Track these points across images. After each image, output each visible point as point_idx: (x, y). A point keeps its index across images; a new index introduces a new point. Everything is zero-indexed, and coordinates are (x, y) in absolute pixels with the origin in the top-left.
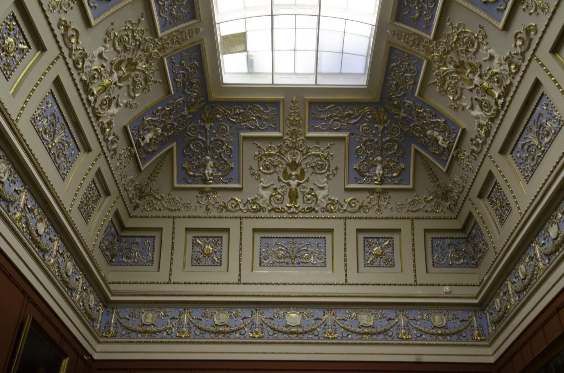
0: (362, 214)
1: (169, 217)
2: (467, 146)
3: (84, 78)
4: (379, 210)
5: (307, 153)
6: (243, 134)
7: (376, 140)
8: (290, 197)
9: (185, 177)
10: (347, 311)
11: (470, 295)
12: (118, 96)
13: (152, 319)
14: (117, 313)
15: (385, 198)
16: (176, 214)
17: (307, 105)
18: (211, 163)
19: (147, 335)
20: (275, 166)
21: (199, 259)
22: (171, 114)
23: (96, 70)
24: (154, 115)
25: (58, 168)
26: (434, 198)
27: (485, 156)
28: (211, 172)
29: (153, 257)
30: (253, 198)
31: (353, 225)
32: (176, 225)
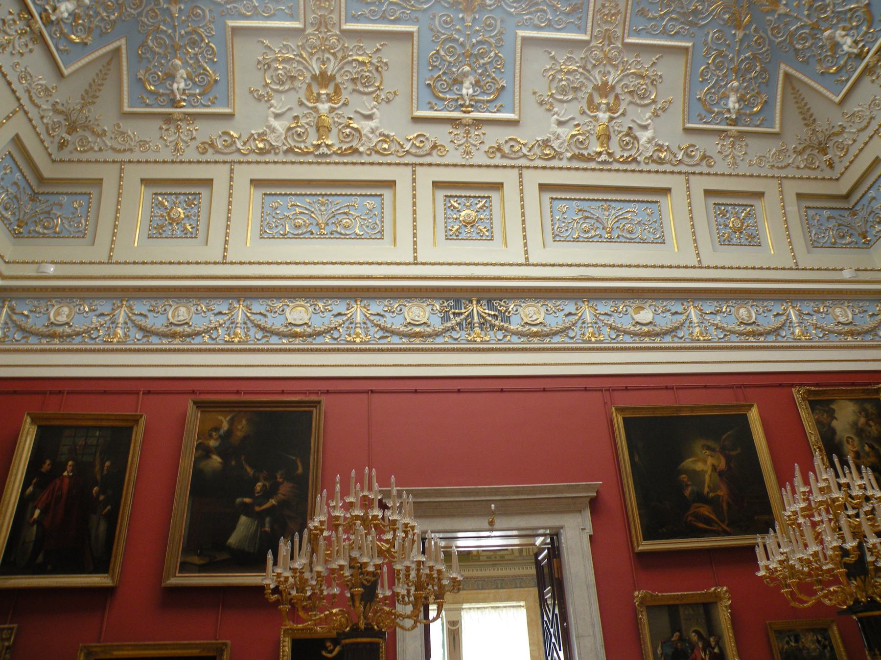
1: (114, 162)
5: (344, 58)
13: (68, 316)
14: (12, 309)
16: (126, 157)
19: (56, 341)
29: (86, 225)
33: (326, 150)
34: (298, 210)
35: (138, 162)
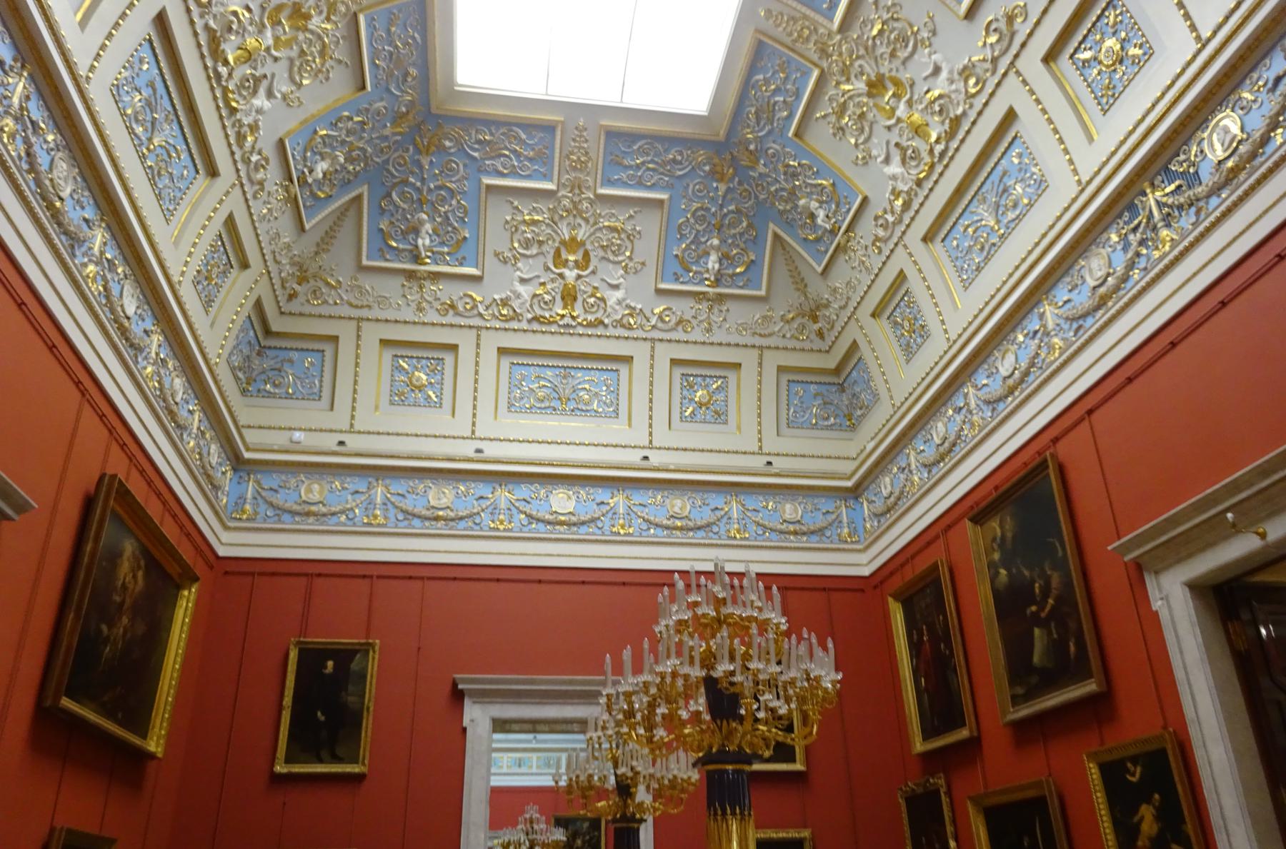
1: (350, 318)
2: (867, 229)
3: (212, 23)
4: (709, 330)
5: (595, 223)
6: (487, 181)
8: (563, 298)
9: (383, 250)
11: (846, 471)
12: (273, 75)
16: (364, 313)
17: (603, 137)
18: (428, 227)
19: (311, 520)
21: (403, 394)
22: (363, 130)
23: (235, 13)
24: (334, 126)
25: (159, 197)
26: (798, 315)
27: (896, 245)
28: (427, 242)
30: (504, 296)
31: (665, 353)
32: (363, 334)
34: (542, 383)
35: (377, 320)
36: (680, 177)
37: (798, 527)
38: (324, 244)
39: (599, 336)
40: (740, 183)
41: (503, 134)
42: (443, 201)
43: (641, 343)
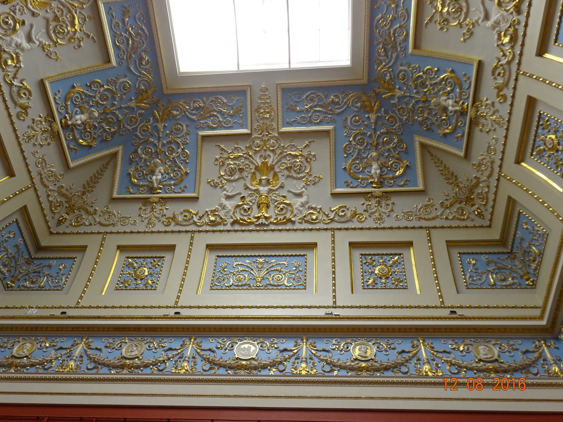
0: (355, 224)
7: (369, 133)
10: (334, 342)
15: (388, 205)
16: (109, 229)
20: (241, 170)
28: (160, 177)
29: (66, 281)
32: (105, 243)
33: (264, 221)
34: (241, 268)
36: (339, 114)
37: (496, 365)
38: (90, 186)
39: (288, 230)
40: (386, 112)
41: (212, 101)
42: (172, 151)
43: (323, 233)
